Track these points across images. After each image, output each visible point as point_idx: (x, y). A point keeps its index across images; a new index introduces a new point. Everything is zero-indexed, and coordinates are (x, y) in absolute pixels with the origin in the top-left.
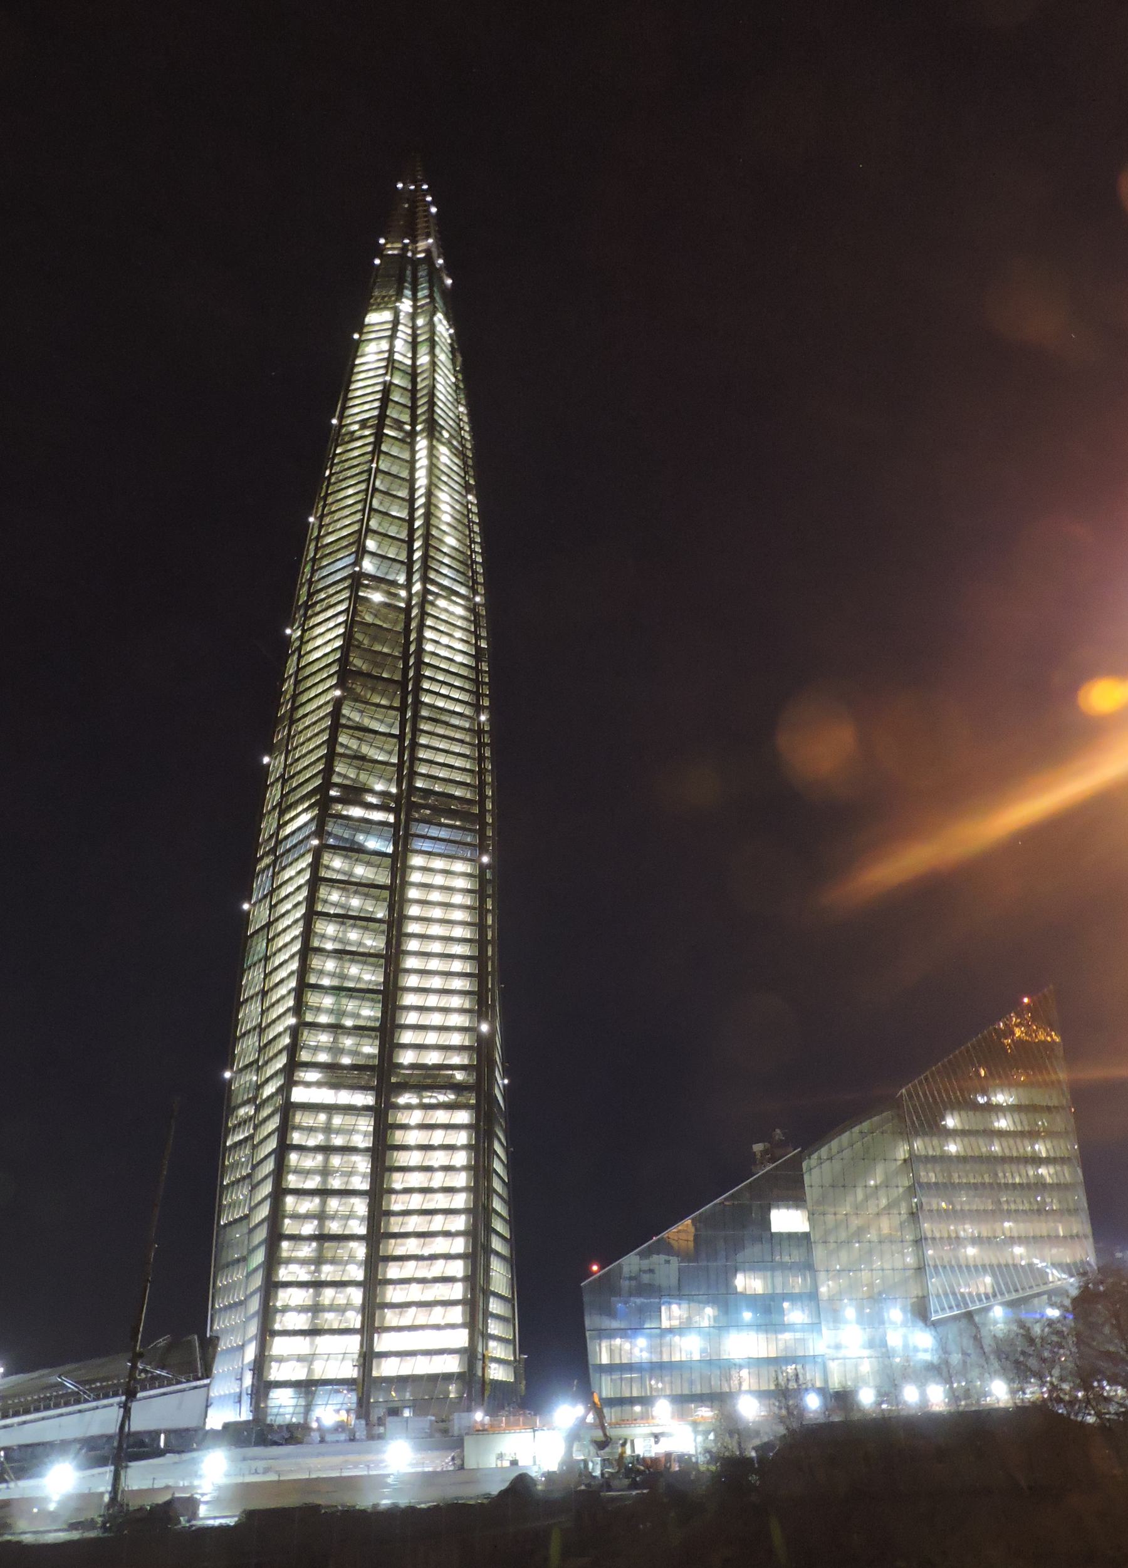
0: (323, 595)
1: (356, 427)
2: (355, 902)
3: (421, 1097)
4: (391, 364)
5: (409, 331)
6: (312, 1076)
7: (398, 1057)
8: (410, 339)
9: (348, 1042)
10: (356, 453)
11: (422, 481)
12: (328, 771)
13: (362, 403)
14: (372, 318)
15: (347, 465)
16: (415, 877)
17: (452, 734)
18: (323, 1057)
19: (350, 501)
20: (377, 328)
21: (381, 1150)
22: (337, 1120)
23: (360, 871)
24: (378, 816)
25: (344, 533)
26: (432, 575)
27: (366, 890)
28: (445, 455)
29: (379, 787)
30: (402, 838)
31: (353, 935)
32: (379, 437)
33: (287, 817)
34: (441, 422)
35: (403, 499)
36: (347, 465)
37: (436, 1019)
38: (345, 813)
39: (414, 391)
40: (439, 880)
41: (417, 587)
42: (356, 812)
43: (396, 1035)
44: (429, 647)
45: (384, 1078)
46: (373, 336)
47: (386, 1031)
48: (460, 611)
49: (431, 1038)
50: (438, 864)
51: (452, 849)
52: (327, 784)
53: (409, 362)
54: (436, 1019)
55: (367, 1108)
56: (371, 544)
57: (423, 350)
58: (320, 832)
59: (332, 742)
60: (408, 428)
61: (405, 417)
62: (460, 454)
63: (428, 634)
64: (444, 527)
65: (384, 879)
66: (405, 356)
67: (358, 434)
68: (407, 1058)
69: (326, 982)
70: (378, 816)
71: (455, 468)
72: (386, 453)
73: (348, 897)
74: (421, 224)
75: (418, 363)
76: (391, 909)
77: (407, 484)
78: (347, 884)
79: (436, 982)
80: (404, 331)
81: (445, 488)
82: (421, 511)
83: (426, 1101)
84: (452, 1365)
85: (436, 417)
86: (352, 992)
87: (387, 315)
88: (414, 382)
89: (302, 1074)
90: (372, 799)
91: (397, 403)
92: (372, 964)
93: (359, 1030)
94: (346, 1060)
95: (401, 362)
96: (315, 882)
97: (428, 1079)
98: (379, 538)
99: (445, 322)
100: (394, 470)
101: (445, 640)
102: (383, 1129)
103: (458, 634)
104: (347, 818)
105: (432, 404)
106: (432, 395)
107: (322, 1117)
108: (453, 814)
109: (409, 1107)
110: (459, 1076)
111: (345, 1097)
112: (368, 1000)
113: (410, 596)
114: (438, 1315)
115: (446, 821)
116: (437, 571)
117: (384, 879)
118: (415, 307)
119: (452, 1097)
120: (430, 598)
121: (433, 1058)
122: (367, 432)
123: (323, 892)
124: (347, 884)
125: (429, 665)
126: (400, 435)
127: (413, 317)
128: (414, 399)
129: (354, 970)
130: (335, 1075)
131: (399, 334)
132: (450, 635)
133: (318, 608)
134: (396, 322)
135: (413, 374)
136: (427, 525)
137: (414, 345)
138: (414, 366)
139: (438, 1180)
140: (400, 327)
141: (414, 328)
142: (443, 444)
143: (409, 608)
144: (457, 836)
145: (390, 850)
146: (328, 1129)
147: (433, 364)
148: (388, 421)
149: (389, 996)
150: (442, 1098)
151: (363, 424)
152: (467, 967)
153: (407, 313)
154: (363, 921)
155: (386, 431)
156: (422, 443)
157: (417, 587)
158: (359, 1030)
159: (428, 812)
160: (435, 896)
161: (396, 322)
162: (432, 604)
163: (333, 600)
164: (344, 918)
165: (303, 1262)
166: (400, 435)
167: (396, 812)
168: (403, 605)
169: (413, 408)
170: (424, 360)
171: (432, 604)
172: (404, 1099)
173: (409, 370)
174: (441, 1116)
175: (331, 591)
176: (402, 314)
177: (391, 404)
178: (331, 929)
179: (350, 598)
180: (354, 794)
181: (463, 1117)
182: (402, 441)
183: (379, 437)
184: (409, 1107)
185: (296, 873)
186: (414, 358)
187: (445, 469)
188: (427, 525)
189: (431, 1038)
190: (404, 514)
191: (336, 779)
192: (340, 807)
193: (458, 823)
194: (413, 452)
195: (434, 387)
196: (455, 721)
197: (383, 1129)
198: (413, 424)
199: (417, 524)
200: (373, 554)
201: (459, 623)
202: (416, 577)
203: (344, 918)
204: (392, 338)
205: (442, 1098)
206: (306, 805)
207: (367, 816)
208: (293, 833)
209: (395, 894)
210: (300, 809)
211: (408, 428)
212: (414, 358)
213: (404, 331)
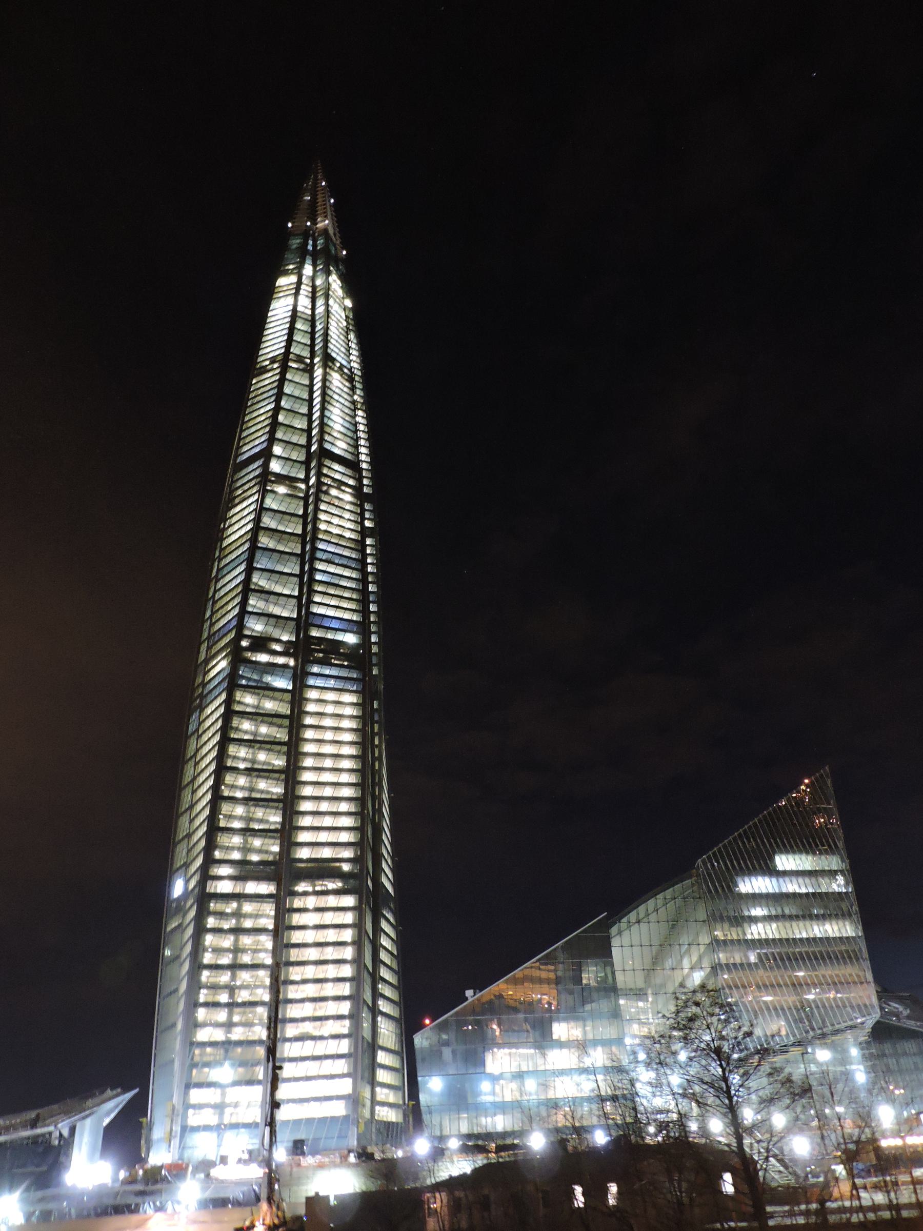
0: (240, 492)
1: (267, 363)
2: (264, 730)
3: (314, 886)
4: (295, 315)
5: (310, 289)
6: (224, 871)
7: (295, 853)
8: (310, 295)
9: (257, 843)
10: (267, 382)
11: (317, 400)
12: (240, 626)
13: (273, 343)
14: (282, 281)
15: (260, 392)
16: (311, 707)
17: (341, 594)
18: (236, 856)
19: (263, 418)
20: (285, 288)
21: (281, 929)
22: (248, 908)
23: (269, 705)
24: (281, 660)
25: (257, 442)
26: (325, 471)
27: (270, 719)
28: (337, 381)
29: (285, 638)
30: (300, 678)
31: (262, 756)
32: (284, 368)
34: (334, 355)
35: (303, 415)
36: (260, 392)
37: (328, 821)
38: (254, 659)
39: (313, 333)
40: (330, 709)
41: (312, 481)
42: (263, 658)
43: (293, 835)
44: (323, 526)
45: (285, 873)
46: (281, 294)
48: (348, 498)
49: (323, 837)
50: (330, 696)
51: (340, 685)
52: (240, 636)
53: (309, 312)
54: (328, 821)
55: (270, 896)
56: (277, 450)
57: (320, 302)
59: (244, 603)
60: (308, 361)
61: (306, 353)
62: (351, 379)
63: (322, 516)
64: (335, 434)
65: (285, 709)
66: (306, 307)
67: (269, 367)
68: (304, 853)
69: (239, 794)
70: (281, 660)
71: (346, 389)
72: (290, 381)
73: (257, 726)
74: (320, 209)
75: (317, 312)
76: (290, 734)
77: (307, 403)
78: (258, 716)
79: (328, 792)
80: (305, 289)
81: (338, 405)
82: (317, 423)
83: (318, 888)
84: (339, 1109)
85: (329, 351)
86: (257, 802)
87: (293, 279)
88: (313, 326)
89: (216, 870)
90: (277, 647)
91: (299, 342)
92: (274, 779)
93: (264, 833)
94: (255, 858)
95: (303, 313)
96: (229, 714)
97: (321, 870)
98: (283, 445)
99: (339, 282)
100: (297, 393)
101: (335, 520)
102: (282, 913)
103: (347, 515)
104: (256, 663)
105: (326, 341)
106: (326, 335)
107: (234, 905)
108: (340, 656)
109: (305, 894)
110: (346, 867)
111: (251, 887)
112: (272, 807)
113: (308, 488)
114: (329, 1067)
115: (336, 662)
116: (329, 468)
117: (285, 709)
118: (315, 271)
119: (340, 884)
120: (325, 488)
121: (327, 853)
122: (276, 366)
123: (235, 722)
124: (258, 716)
125: (322, 540)
126: (302, 366)
127: (313, 279)
128: (313, 339)
129: (262, 785)
130: (246, 871)
131: (302, 292)
132: (341, 517)
133: (237, 501)
134: (299, 283)
135: (313, 322)
136: (322, 432)
138: (313, 315)
139: (330, 953)
140: (303, 287)
141: (314, 287)
142: (336, 371)
144: (344, 673)
145: (290, 687)
146: (238, 914)
147: (328, 312)
148: (291, 356)
149: (288, 804)
150: (331, 886)
151: (273, 360)
152: (352, 779)
153: (308, 277)
154: (268, 744)
155: (290, 364)
156: (318, 373)
157: (312, 481)
158: (264, 833)
159: (321, 655)
160: (327, 722)
161: (299, 283)
162: (326, 493)
163: (249, 493)
164: (254, 743)
165: (217, 1025)
166: (302, 366)
167: (294, 655)
168: (302, 495)
169: (312, 346)
170: (320, 310)
171: (326, 493)
172: (302, 887)
173: (310, 318)
174: (332, 901)
175: (246, 487)
176: (304, 277)
177: (294, 344)
178: (243, 752)
179: (259, 491)
180: (261, 643)
181: (349, 901)
182: (304, 370)
183: (284, 368)
184: (305, 894)
185: (214, 710)
186: (313, 309)
187: (337, 391)
188: (322, 432)
189: (323, 837)
190: (305, 426)
191: (247, 632)
192: (248, 654)
193: (346, 663)
194: (312, 379)
195: (328, 328)
196: (344, 583)
197: (282, 913)
198: (312, 357)
199: (314, 432)
200: (279, 457)
201: (348, 507)
202: (313, 473)
203: (254, 743)
204: (297, 294)
205: (331, 886)
207: (271, 661)
208: (214, 677)
209: (295, 722)
210: (219, 658)
211: (308, 361)
212: (313, 309)
213: (305, 289)
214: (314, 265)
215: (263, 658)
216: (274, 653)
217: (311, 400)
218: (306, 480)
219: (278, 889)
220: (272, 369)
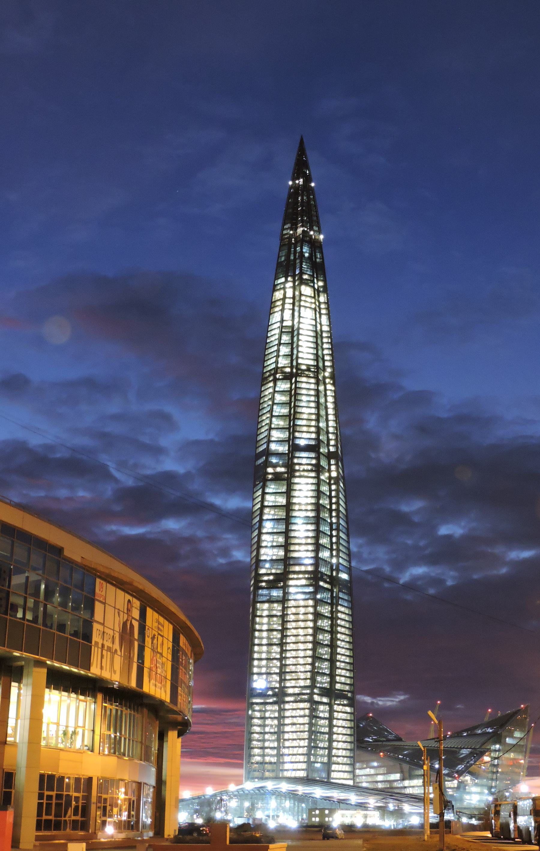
1: (304, 367)
11: (331, 411)
33: (291, 576)
42: (321, 583)
47: (332, 676)
58: (315, 593)
97: (341, 695)
113: (330, 478)
137: (320, 314)
138: (322, 332)
143: (330, 484)
150: (345, 702)
156: (329, 387)
181: (348, 709)
197: (331, 711)
202: (333, 468)
206: (307, 576)
214: (318, 280)
215: (321, 583)
216: (326, 582)
217: (326, 408)
218: (329, 471)
219: (330, 701)
220: (308, 377)
